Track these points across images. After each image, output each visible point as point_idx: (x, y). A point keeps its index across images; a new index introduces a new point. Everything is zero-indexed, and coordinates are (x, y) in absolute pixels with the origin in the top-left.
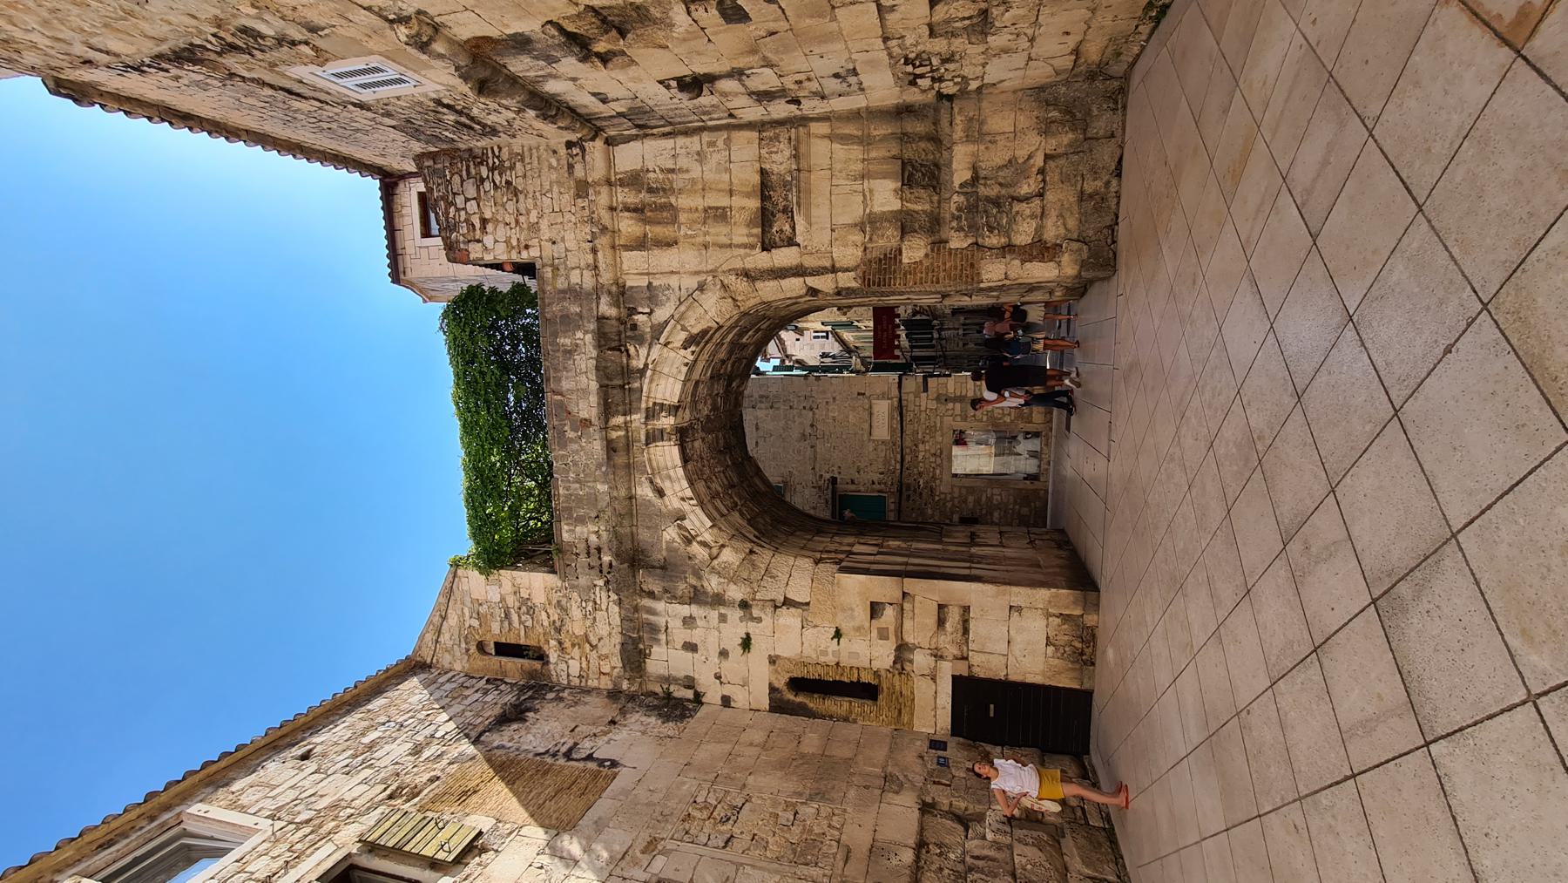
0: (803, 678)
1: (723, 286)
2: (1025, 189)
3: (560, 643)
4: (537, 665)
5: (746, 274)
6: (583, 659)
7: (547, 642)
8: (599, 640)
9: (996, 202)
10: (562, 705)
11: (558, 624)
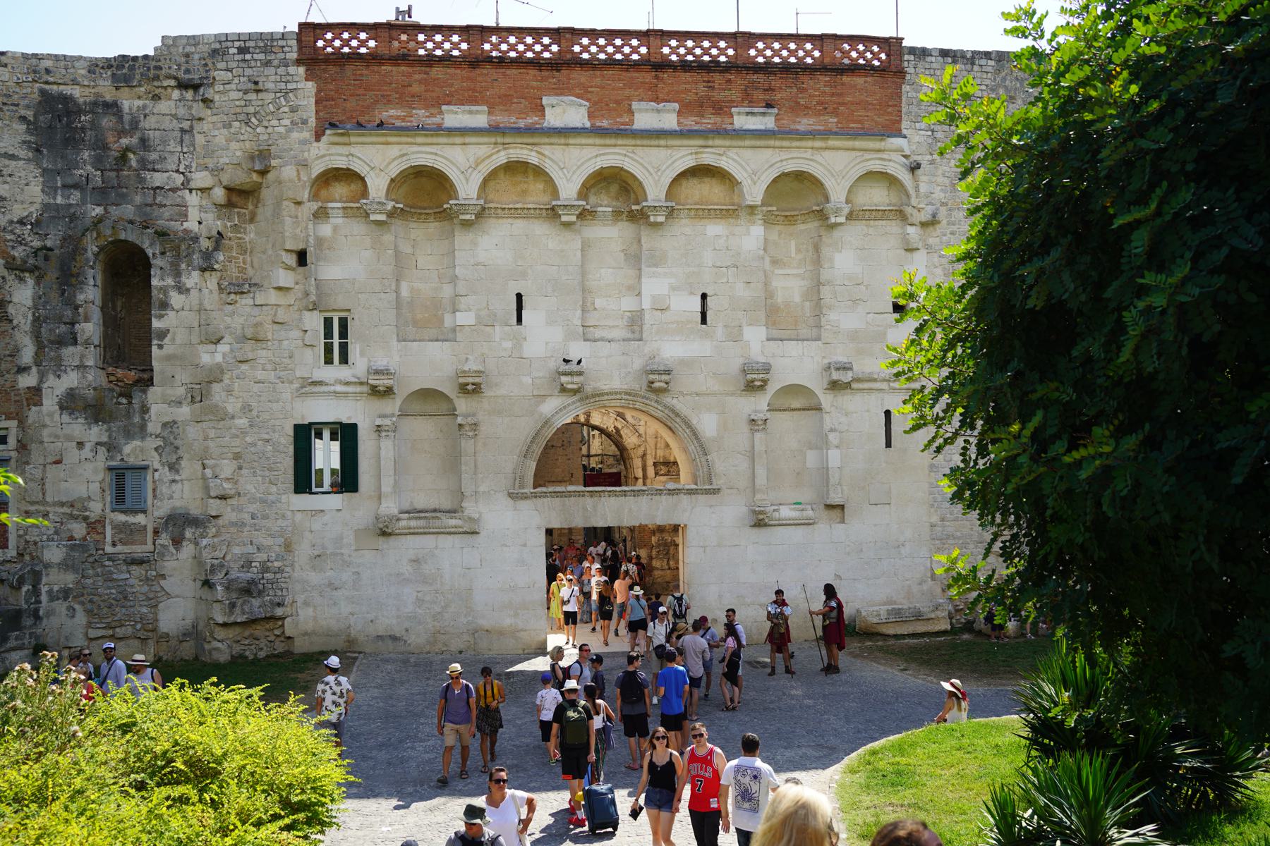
1: (639, 446)
2: (671, 563)
5: (644, 455)
9: (667, 553)
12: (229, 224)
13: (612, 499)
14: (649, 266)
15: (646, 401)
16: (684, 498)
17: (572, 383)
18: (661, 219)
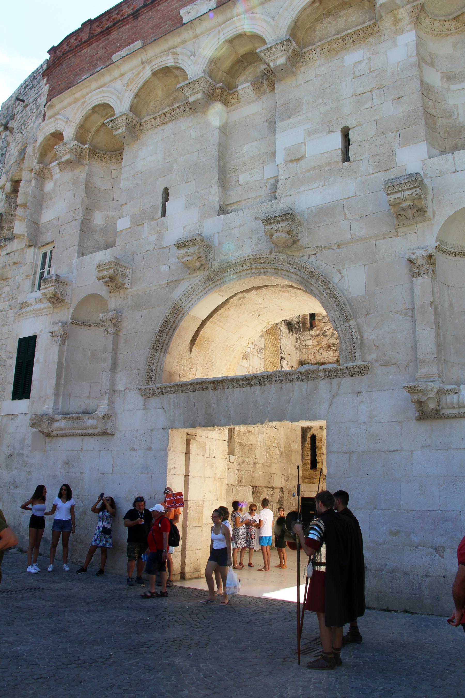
0: (316, 440)
3: (318, 335)
4: (308, 325)
6: (313, 346)
7: (318, 330)
8: (321, 353)
10: (295, 343)
11: (326, 334)
12: (13, 206)
13: (237, 390)
14: (284, 120)
15: (276, 266)
16: (323, 385)
17: (187, 255)
18: (281, 61)
